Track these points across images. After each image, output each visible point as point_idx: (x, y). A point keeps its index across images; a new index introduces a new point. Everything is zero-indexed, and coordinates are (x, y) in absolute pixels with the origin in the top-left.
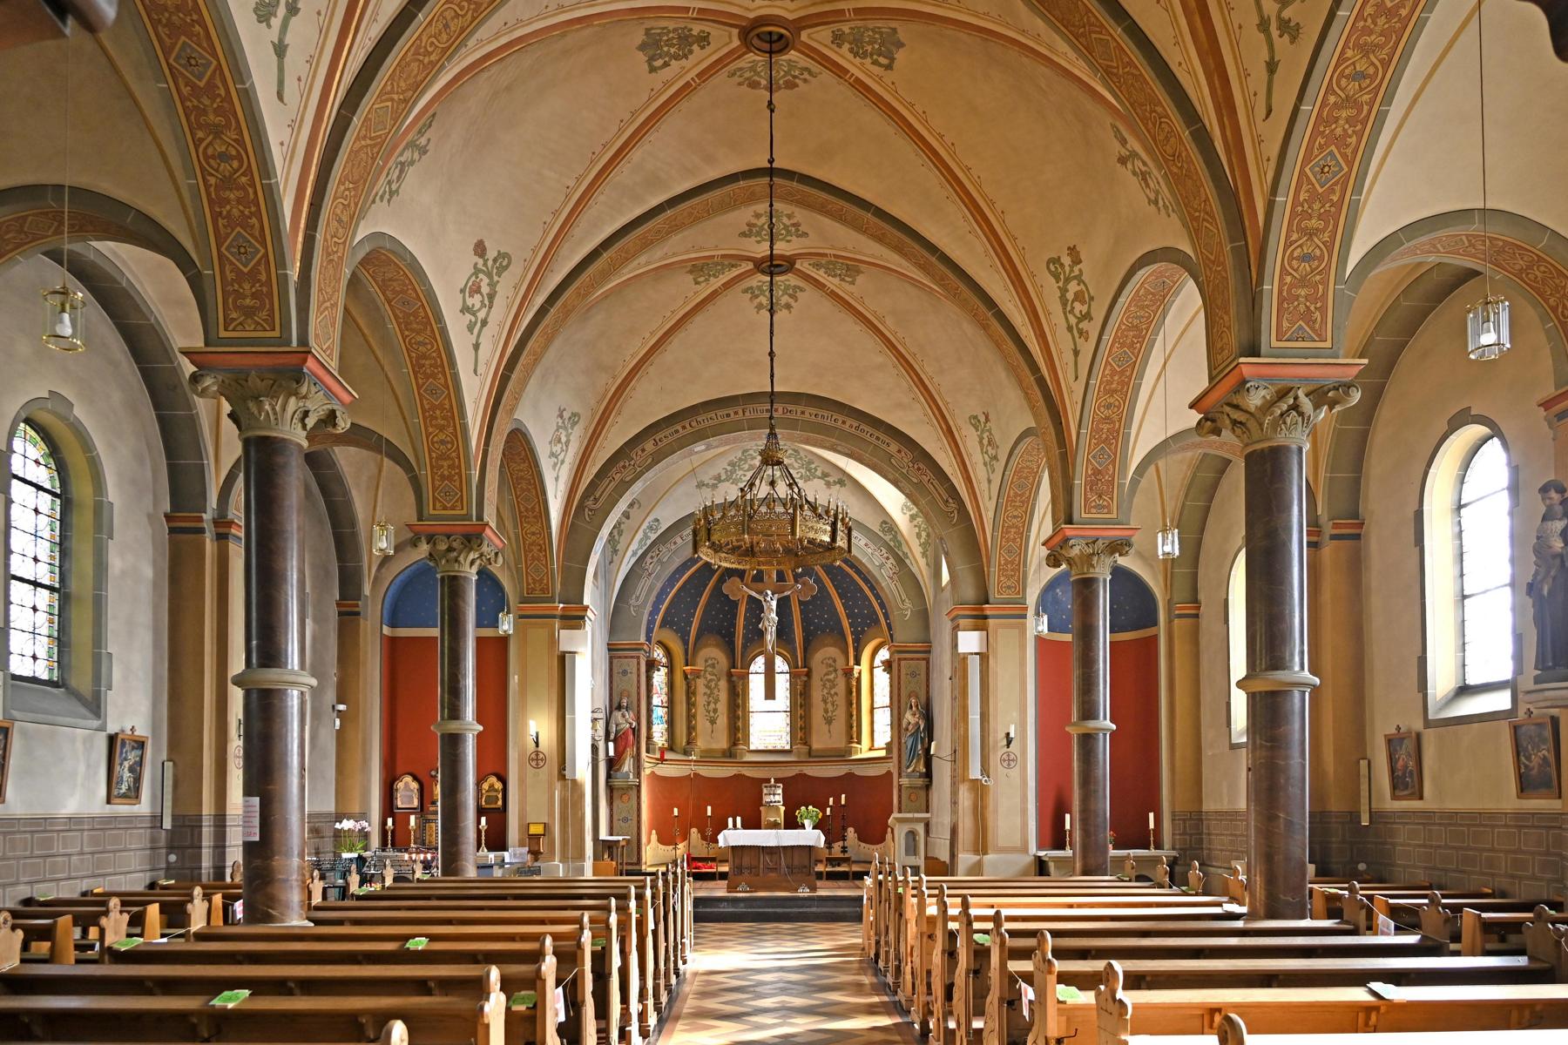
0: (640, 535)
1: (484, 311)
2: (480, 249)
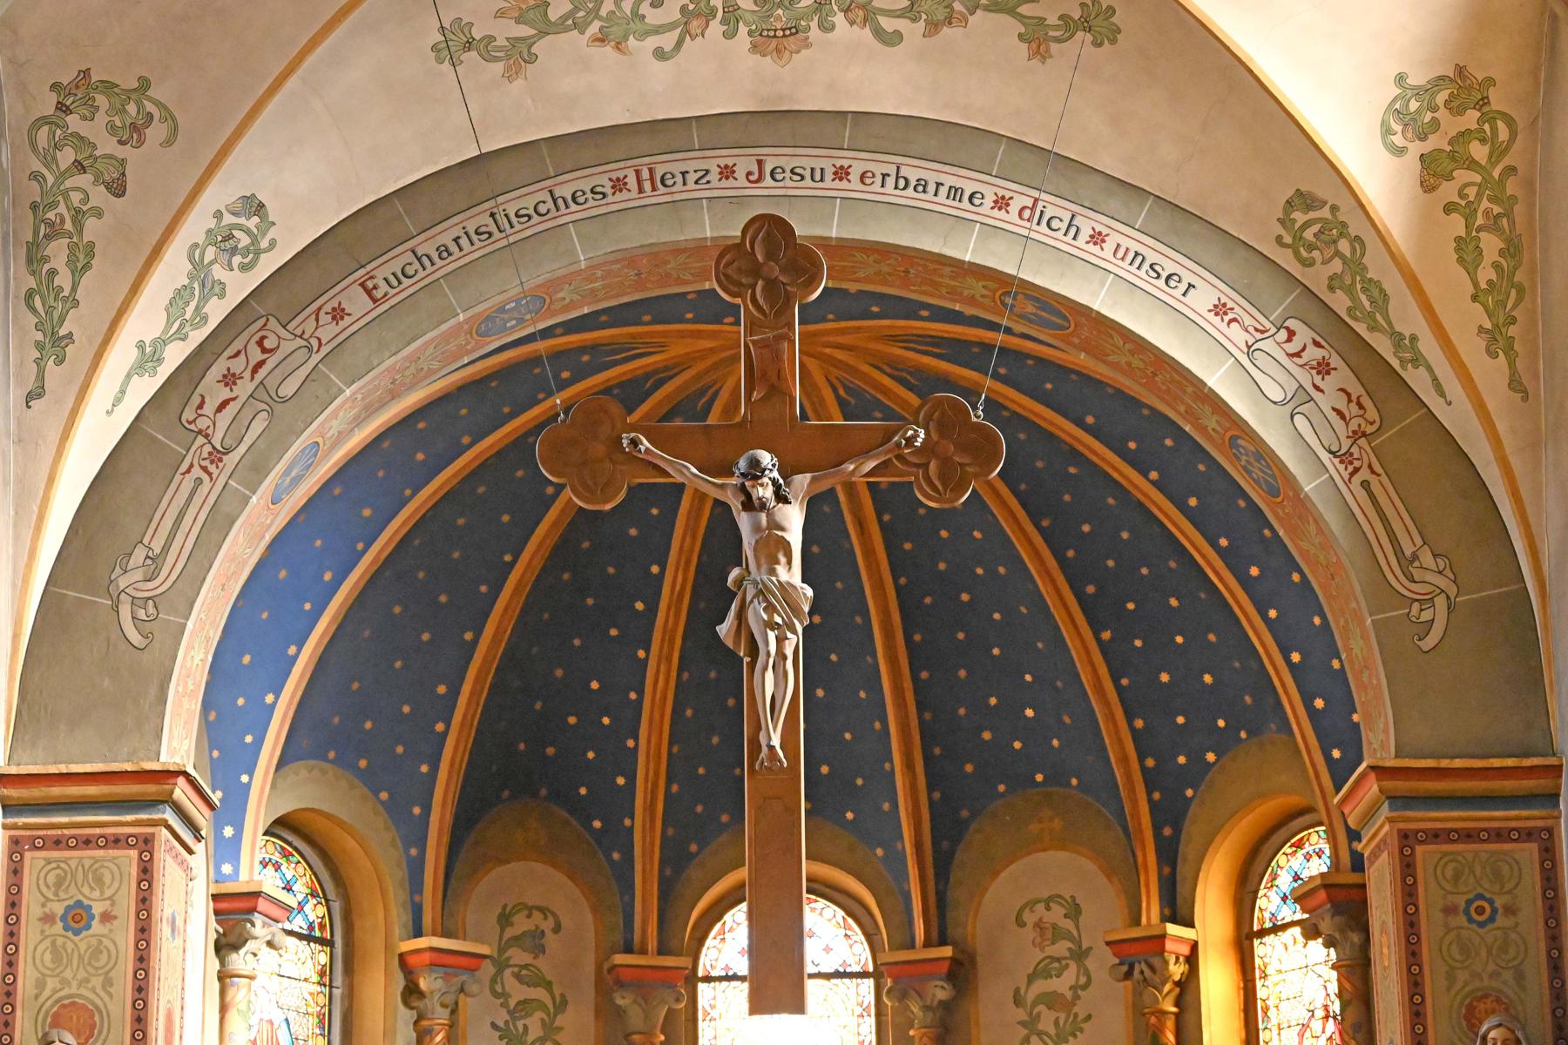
0: (172, 270)
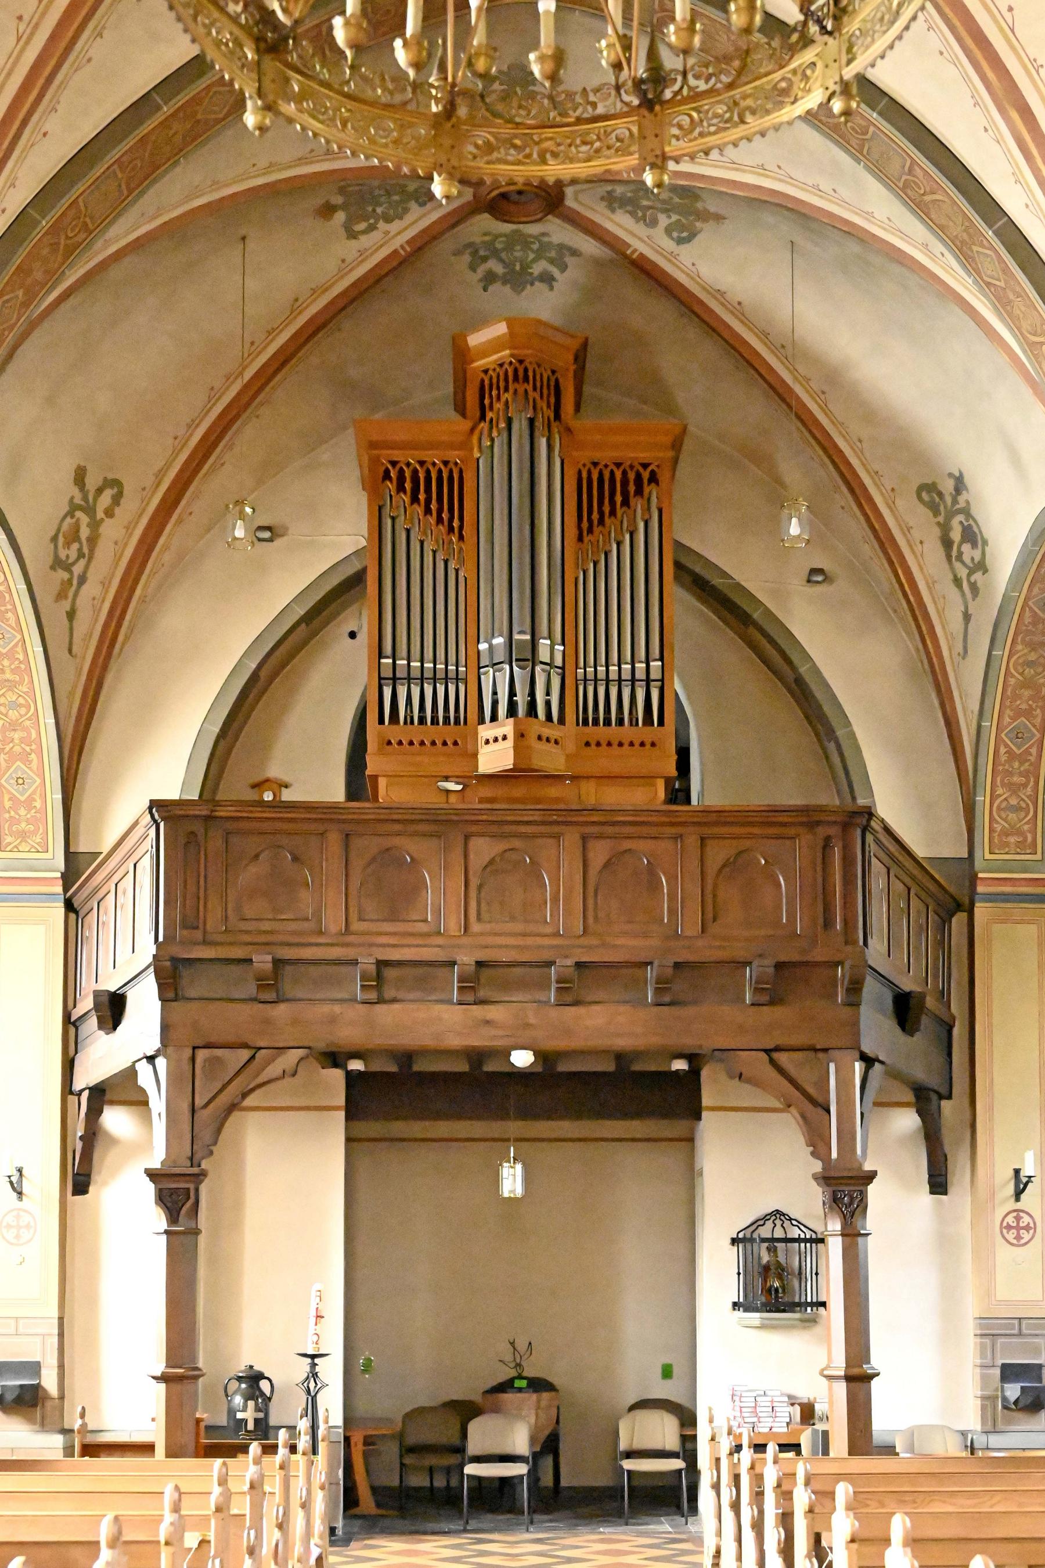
1: (82, 563)
2: (80, 477)
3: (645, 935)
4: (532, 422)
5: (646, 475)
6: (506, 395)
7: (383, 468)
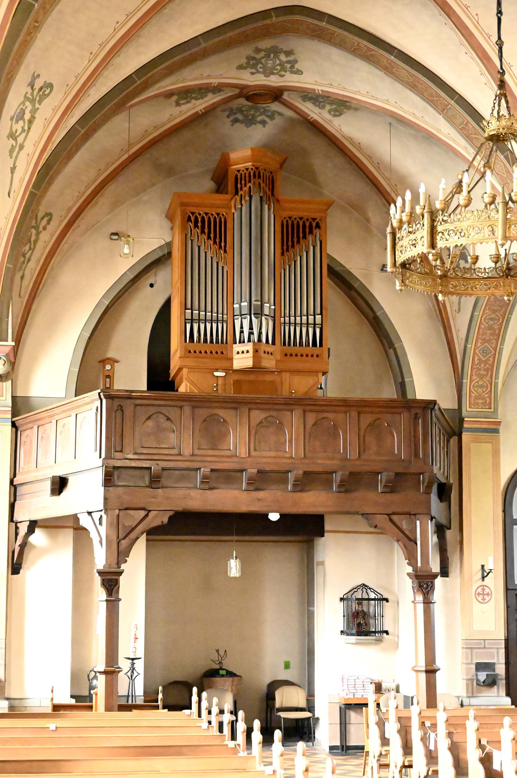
3: (332, 459)
4: (261, 197)
5: (314, 224)
6: (250, 184)
7: (187, 216)
